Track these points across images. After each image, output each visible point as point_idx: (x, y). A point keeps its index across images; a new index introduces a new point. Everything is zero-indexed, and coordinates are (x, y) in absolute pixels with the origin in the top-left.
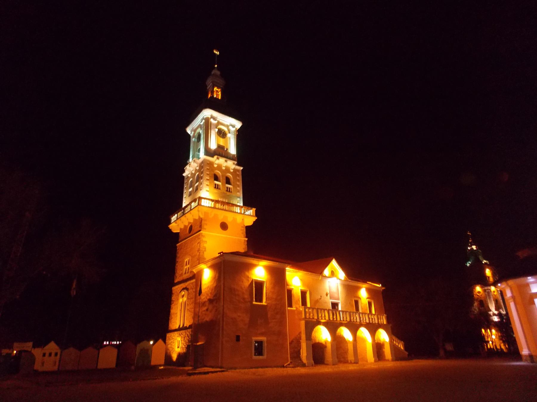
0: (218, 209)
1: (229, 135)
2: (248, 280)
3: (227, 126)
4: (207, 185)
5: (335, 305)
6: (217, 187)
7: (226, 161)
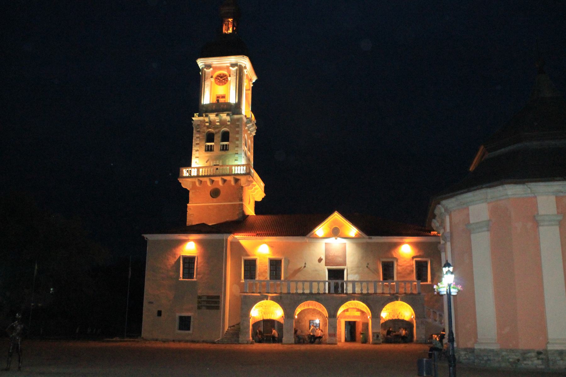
0: (202, 176)
1: (229, 78)
2: (175, 258)
3: (228, 67)
4: (197, 151)
5: (336, 274)
6: (209, 149)
7: (217, 115)
